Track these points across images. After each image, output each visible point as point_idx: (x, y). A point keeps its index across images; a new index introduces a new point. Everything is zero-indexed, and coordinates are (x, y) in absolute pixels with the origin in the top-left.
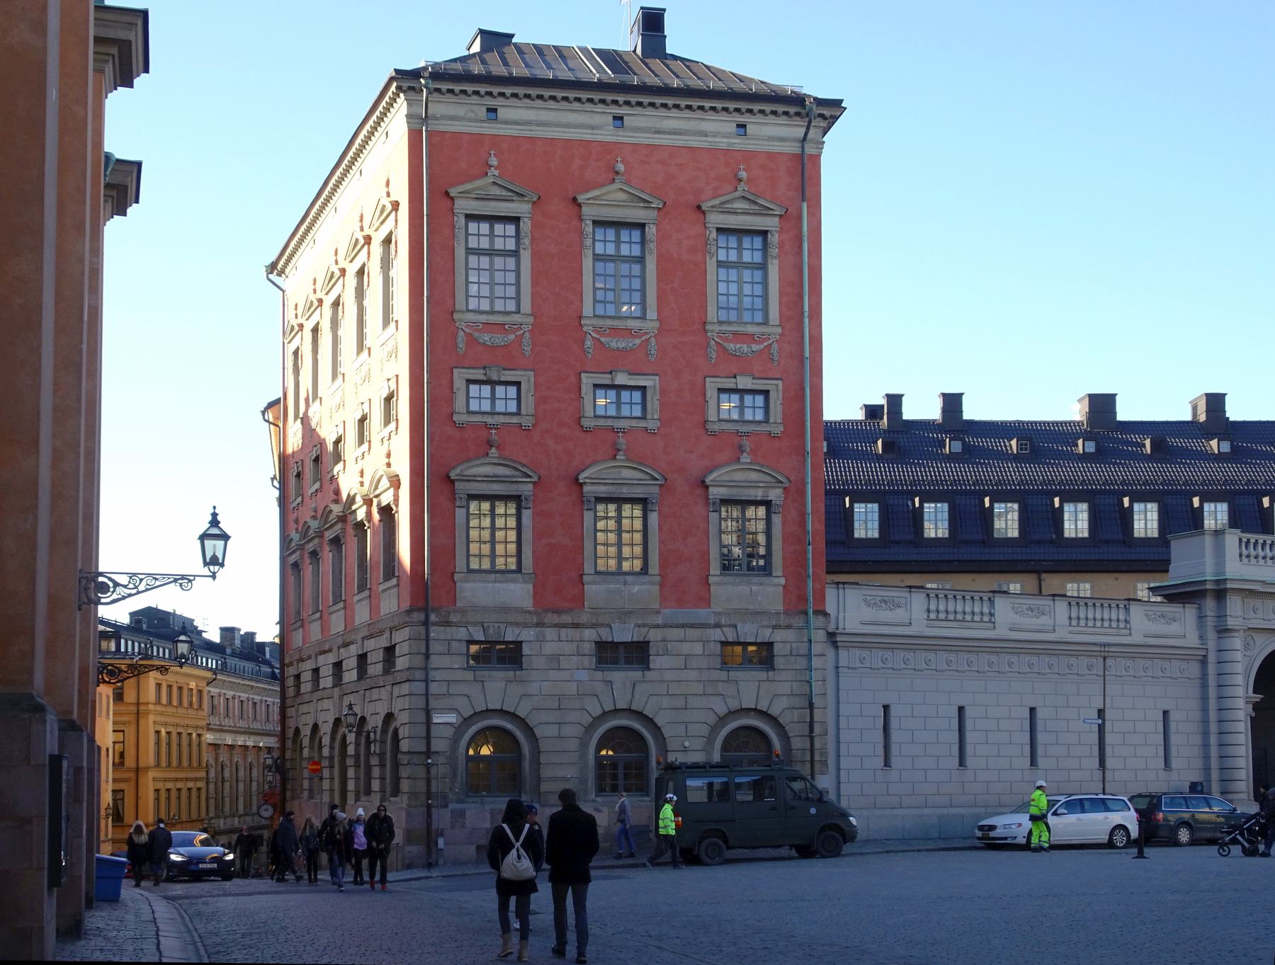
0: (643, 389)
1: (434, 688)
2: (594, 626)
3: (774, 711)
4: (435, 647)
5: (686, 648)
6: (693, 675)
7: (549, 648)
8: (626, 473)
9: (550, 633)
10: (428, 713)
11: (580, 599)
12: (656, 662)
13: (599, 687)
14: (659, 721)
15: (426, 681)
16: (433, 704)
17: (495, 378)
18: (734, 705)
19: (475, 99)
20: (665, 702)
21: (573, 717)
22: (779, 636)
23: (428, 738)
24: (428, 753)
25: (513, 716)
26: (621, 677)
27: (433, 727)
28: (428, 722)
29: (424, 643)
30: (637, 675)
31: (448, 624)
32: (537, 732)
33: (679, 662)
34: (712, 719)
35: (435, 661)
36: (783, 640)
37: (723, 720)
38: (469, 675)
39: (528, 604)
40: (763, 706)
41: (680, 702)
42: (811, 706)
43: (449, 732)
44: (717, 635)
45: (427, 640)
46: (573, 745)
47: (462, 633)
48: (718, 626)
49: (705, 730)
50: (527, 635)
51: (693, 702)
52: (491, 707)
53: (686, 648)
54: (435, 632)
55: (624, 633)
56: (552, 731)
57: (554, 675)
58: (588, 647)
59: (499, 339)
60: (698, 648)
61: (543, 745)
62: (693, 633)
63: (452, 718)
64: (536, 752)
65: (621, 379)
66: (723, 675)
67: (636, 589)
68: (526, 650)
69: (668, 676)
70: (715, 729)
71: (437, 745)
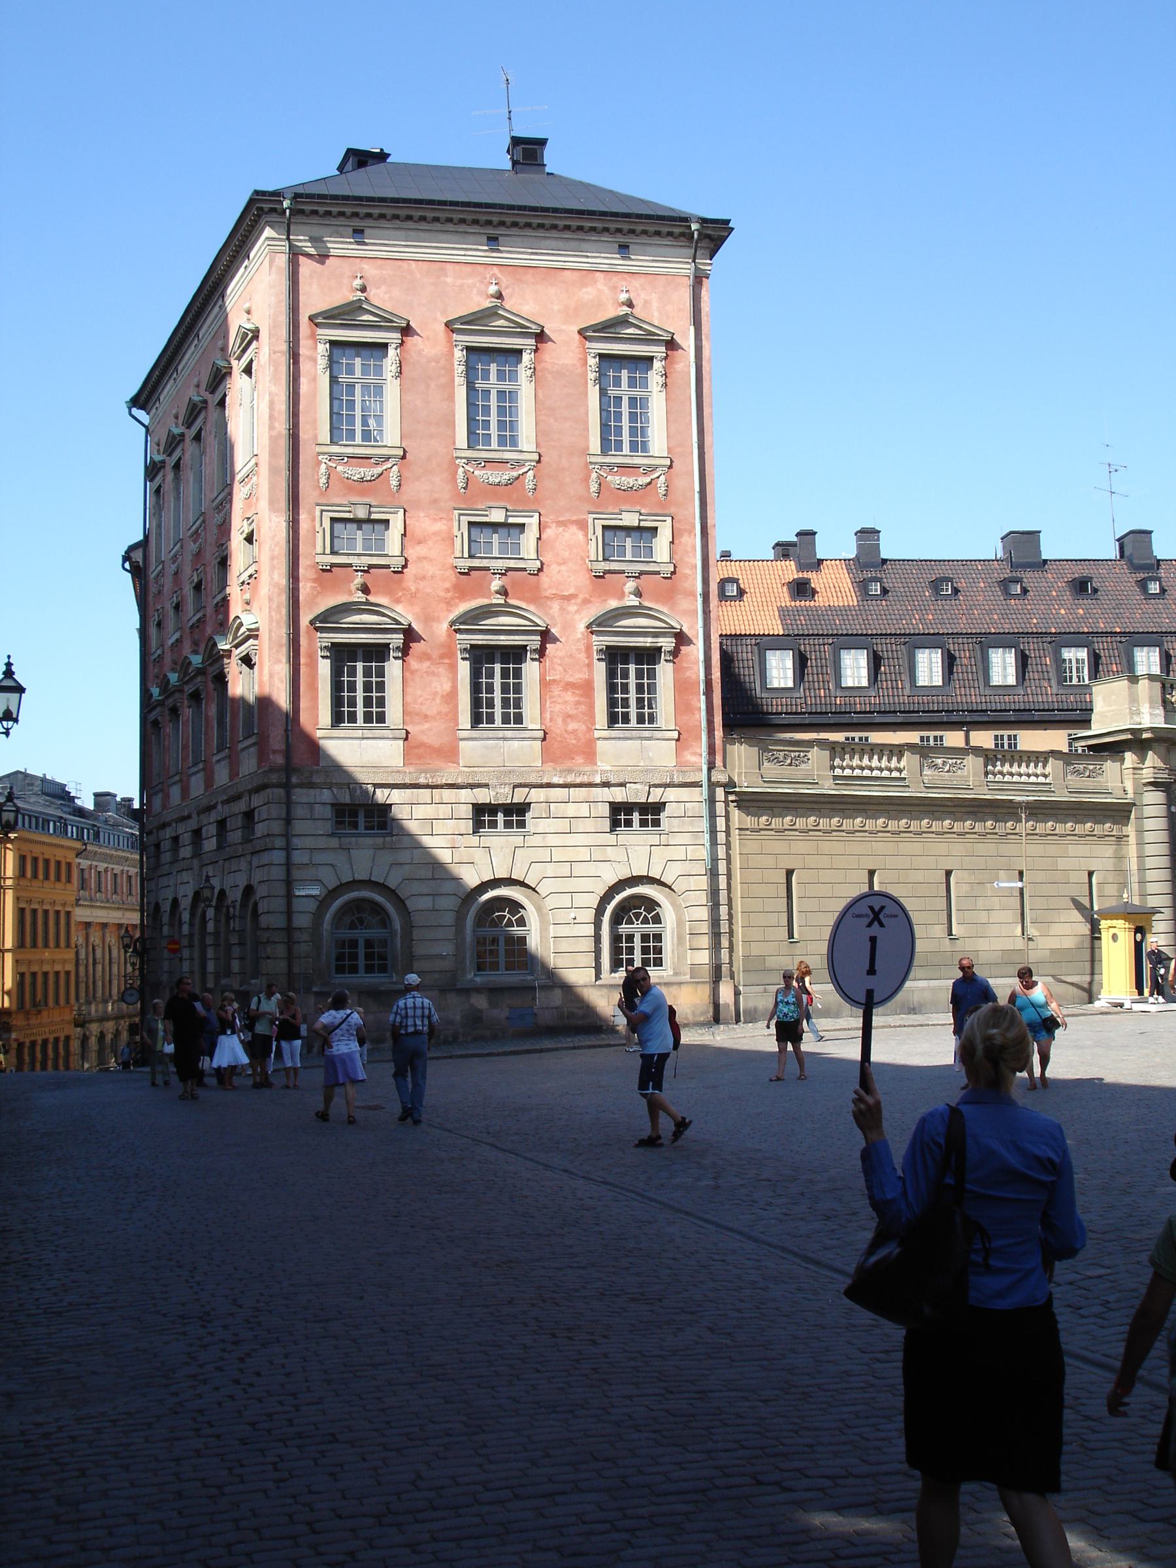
1: (298, 857)
10: (289, 883)
15: (288, 849)
16: (296, 874)
19: (342, 221)
23: (289, 913)
24: (289, 929)
25: (382, 887)
27: (294, 900)
28: (289, 896)
29: (284, 806)
31: (311, 785)
35: (299, 827)
38: (334, 843)
43: (312, 906)
45: (289, 804)
46: (449, 918)
47: (326, 795)
52: (358, 877)
58: (467, 811)
61: (418, 920)
63: (315, 891)
64: (409, 926)
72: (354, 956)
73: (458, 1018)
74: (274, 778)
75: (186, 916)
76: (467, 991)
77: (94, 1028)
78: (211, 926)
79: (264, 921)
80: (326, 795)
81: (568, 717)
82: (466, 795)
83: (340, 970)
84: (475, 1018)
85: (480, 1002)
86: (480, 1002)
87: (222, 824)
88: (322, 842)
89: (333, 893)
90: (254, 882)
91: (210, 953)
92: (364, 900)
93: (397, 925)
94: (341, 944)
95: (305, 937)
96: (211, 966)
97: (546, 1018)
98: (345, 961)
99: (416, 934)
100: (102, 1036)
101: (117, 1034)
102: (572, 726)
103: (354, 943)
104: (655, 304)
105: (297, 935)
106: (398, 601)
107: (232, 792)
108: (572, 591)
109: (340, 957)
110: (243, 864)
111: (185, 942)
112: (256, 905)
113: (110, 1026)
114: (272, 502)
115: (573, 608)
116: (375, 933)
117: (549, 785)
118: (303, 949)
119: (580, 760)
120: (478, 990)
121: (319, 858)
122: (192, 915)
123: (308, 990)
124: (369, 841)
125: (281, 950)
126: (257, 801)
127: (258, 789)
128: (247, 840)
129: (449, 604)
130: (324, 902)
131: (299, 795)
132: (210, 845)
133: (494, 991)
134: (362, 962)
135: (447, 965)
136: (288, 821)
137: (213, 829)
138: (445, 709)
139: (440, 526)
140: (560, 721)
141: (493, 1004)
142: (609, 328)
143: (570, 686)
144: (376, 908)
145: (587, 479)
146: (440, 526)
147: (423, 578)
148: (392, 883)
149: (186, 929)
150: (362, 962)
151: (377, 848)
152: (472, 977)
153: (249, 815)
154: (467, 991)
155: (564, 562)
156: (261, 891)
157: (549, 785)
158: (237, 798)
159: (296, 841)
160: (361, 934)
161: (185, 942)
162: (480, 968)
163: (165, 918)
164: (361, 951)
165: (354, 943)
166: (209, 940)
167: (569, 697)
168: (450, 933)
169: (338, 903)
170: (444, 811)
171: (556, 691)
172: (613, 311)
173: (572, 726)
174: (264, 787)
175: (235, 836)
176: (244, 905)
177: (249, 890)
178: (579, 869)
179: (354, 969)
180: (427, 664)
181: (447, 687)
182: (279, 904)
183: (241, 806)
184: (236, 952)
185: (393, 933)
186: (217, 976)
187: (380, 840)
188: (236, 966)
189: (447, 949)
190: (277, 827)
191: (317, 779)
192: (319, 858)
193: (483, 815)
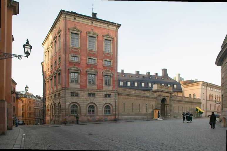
0: (95, 59)
1: (66, 99)
2: (88, 91)
3: (111, 103)
4: (66, 93)
5: (100, 95)
6: (101, 98)
7: (82, 94)
8: (93, 71)
9: (82, 92)
11: (86, 87)
12: (96, 96)
13: (89, 99)
14: (97, 104)
16: (66, 101)
17: (75, 56)
18: (106, 103)
20: (97, 102)
21: (85, 103)
22: (112, 93)
23: (65, 106)
24: (65, 108)
26: (92, 98)
30: (94, 98)
32: (81, 105)
33: (99, 96)
34: (103, 104)
35: (66, 95)
36: (113, 94)
37: (105, 104)
38: (71, 97)
39: (79, 88)
40: (110, 103)
41: (99, 102)
42: (116, 103)
43: (68, 105)
44: (104, 93)
46: (85, 107)
47: (70, 91)
48: (104, 92)
49: (102, 106)
50: (79, 92)
51: (101, 102)
52: (74, 102)
53: (100, 95)
54: (67, 91)
55: (92, 92)
56: (82, 105)
57: (83, 98)
58: (87, 94)
59: (75, 50)
60: (102, 95)
61: (81, 107)
62: (101, 93)
65: (92, 58)
66: (105, 98)
67: (94, 86)
68: (79, 94)
69: (98, 98)
70: (104, 106)
71: (66, 107)
72: (73, 112)
73: (86, 119)
74: (63, 89)
75: (50, 107)
76: (87, 116)
77: (36, 119)
78: (53, 108)
79: (62, 107)
80: (70, 91)
81: (100, 83)
82: (87, 92)
83: (71, 113)
84: (88, 120)
85: (89, 117)
86: (89, 117)
87: (55, 95)
88: (69, 97)
89: (71, 104)
90: (60, 102)
91: (53, 111)
92: (75, 105)
93: (79, 108)
94: (72, 110)
95: (67, 109)
96: (53, 113)
97: (97, 120)
98: (72, 112)
99: (81, 109)
100: (37, 120)
101: (39, 120)
102: (101, 84)
103: (73, 110)
104: (112, 34)
105: (66, 109)
106: (79, 67)
107: (57, 91)
108: (101, 68)
109: (71, 112)
110: (59, 100)
111: (50, 110)
112: (60, 105)
113: (38, 119)
114: (63, 53)
115: (101, 70)
116: (76, 109)
117: (97, 91)
118: (67, 111)
119: (101, 89)
120: (89, 116)
121: (69, 99)
122: (51, 106)
123: (67, 116)
124: (75, 97)
125: (64, 111)
126: (61, 92)
127: (61, 90)
128: (59, 97)
129: (86, 68)
130: (70, 105)
131: (67, 91)
132: (53, 98)
133: (91, 116)
134: (74, 113)
135: (85, 113)
136: (65, 94)
137: (54, 96)
138: (85, 81)
139: (85, 58)
140: (99, 84)
141: (90, 118)
142: (106, 36)
143: (100, 80)
144: (76, 106)
145: (103, 55)
146: (85, 58)
147: (83, 65)
148: (78, 103)
149: (50, 108)
150: (74, 113)
151: (76, 98)
152: (88, 114)
153: (59, 94)
154: (87, 116)
155: (100, 64)
156: (61, 103)
157: (97, 91)
158: (58, 91)
159: (66, 97)
160: (74, 109)
161: (50, 110)
162: (89, 113)
163: (47, 107)
164: (74, 111)
165: (73, 110)
166: (53, 109)
167: (100, 81)
168: (85, 109)
169: (71, 105)
170: (85, 94)
171: (99, 80)
172: (106, 34)
173: (101, 84)
174: (62, 90)
175: (57, 96)
176: (58, 105)
177: (59, 103)
178: (101, 102)
179: (73, 113)
180: (83, 76)
181: (85, 78)
182: (64, 105)
183: (58, 92)
184: (57, 111)
185: (78, 109)
186: (54, 114)
187: (77, 97)
188: (57, 113)
189: (85, 111)
190: (64, 95)
191: (69, 89)
192: (69, 99)
193: (90, 95)
